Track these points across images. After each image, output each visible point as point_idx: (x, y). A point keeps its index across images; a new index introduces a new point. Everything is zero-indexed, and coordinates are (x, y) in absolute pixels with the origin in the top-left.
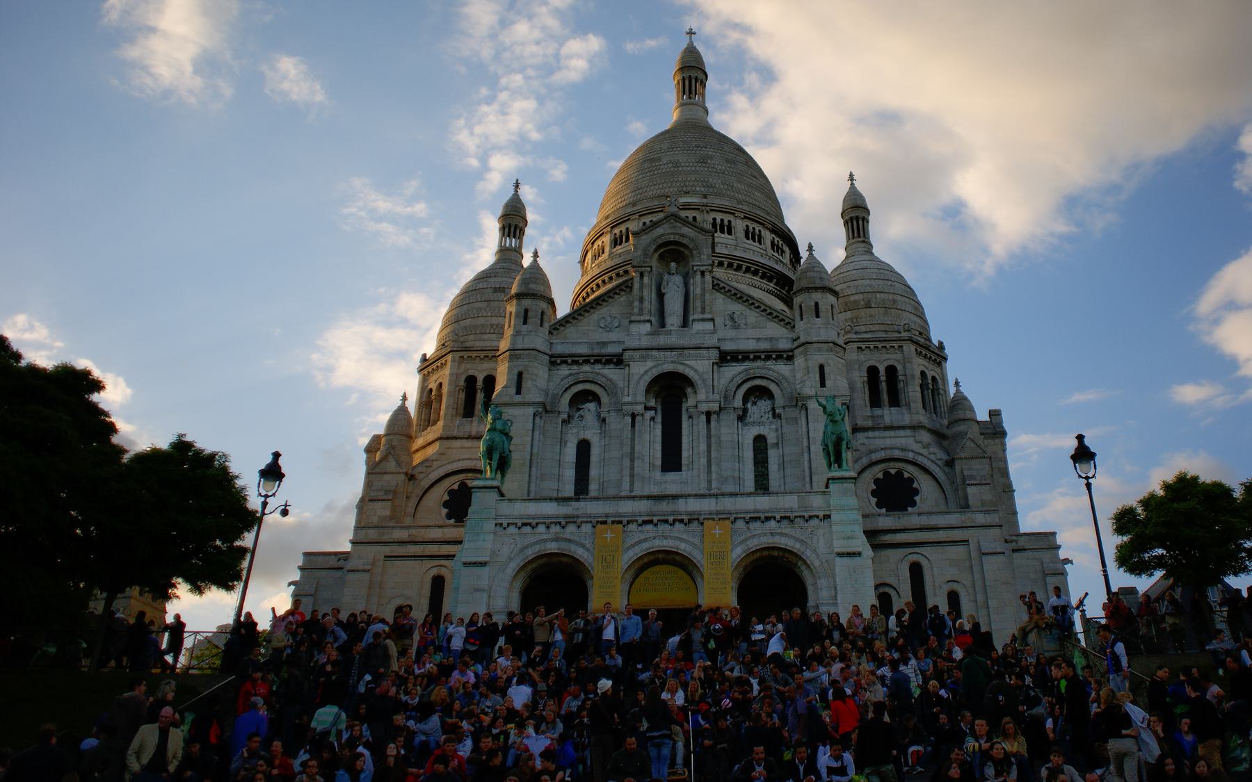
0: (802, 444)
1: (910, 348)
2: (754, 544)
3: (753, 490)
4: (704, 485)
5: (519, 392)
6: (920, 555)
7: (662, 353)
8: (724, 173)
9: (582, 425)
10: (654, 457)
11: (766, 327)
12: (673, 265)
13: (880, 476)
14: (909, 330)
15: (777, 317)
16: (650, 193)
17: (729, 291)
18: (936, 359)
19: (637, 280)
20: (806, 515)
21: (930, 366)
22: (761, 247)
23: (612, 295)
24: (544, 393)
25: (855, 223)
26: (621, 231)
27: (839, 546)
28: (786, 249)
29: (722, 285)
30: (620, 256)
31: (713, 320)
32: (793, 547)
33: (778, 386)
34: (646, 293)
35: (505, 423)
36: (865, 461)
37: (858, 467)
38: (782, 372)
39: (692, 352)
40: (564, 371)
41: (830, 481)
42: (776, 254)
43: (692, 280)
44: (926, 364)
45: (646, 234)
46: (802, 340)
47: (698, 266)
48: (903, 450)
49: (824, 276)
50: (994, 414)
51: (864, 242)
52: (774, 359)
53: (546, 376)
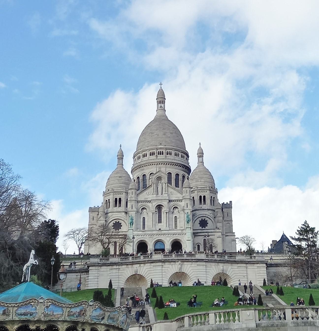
2: (174, 238)
5: (132, 209)
8: (170, 137)
12: (160, 181)
13: (201, 220)
14: (209, 188)
20: (182, 234)
21: (214, 195)
25: (200, 157)
26: (145, 154)
28: (185, 156)
29: (169, 186)
36: (198, 217)
37: (196, 218)
40: (140, 204)
42: (182, 159)
46: (184, 198)
48: (205, 215)
50: (231, 202)
51: (201, 162)
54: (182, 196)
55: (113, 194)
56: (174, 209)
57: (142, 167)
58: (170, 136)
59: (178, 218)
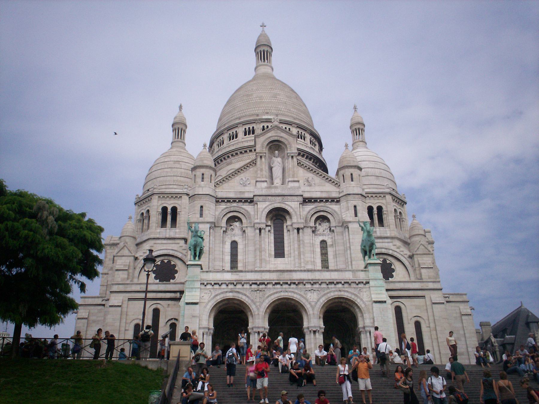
0: (346, 245)
1: (389, 198)
3: (320, 268)
4: (297, 265)
5: (201, 215)
6: (400, 303)
7: (274, 198)
8: (285, 103)
9: (233, 233)
10: (271, 250)
11: (325, 186)
12: (277, 152)
15: (330, 180)
16: (248, 113)
17: (306, 166)
18: (401, 203)
19: (259, 159)
20: (357, 282)
21: (399, 207)
22: (305, 142)
23: (246, 167)
24: (214, 217)
26: (233, 133)
27: (375, 298)
28: (317, 143)
30: (233, 146)
31: (299, 181)
32: (351, 298)
33: (332, 215)
34: (263, 166)
35: (200, 233)
38: (334, 209)
39: (289, 197)
40: (223, 206)
41: (369, 265)
42: (312, 146)
43: (286, 160)
44: (397, 205)
45: (263, 135)
47: (290, 153)
48: (386, 249)
49: (355, 160)
52: (330, 202)
53: (214, 208)
54: (338, 190)
55: (157, 197)
56: (318, 222)
57: (226, 158)
58: (286, 100)
59: (332, 245)
